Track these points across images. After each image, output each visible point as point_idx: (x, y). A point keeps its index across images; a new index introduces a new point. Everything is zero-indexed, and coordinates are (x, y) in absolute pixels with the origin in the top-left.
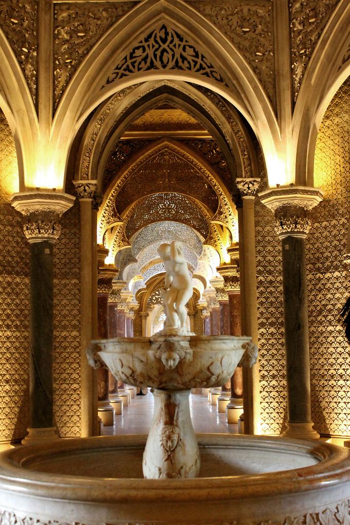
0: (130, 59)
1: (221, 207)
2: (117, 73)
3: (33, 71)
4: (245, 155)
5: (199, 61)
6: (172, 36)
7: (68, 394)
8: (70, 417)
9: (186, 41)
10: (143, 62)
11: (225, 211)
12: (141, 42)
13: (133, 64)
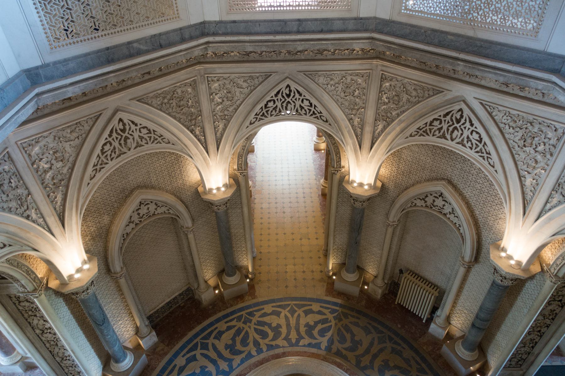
0: (265, 109)
2: (257, 118)
5: (313, 109)
6: (294, 93)
9: (304, 96)
10: (274, 111)
12: (272, 97)
13: (267, 112)
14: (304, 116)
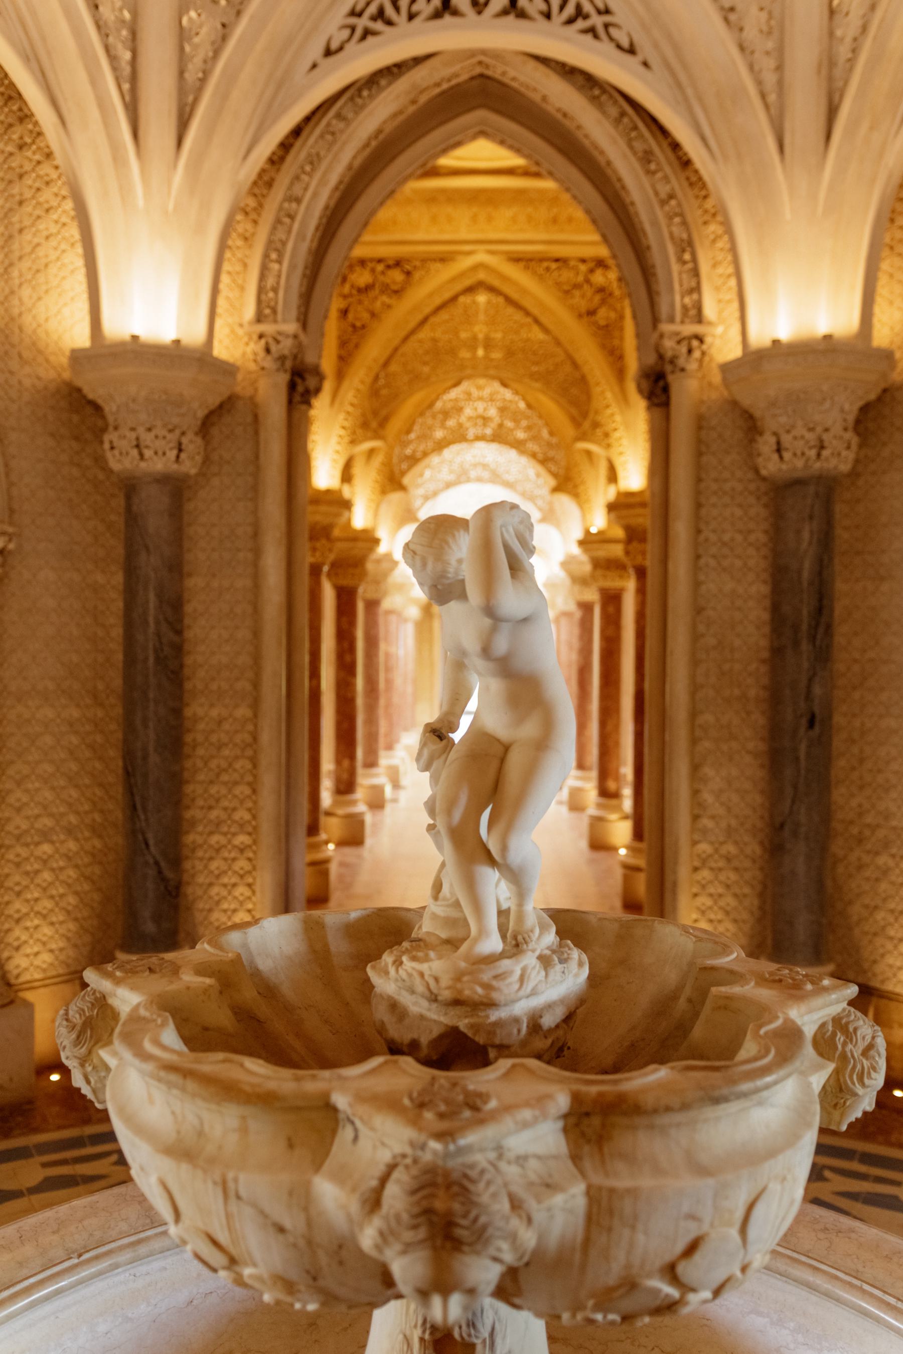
2: (353, 29)
3: (121, 10)
4: (685, 263)
7: (225, 859)
8: (229, 913)
14: (541, 21)
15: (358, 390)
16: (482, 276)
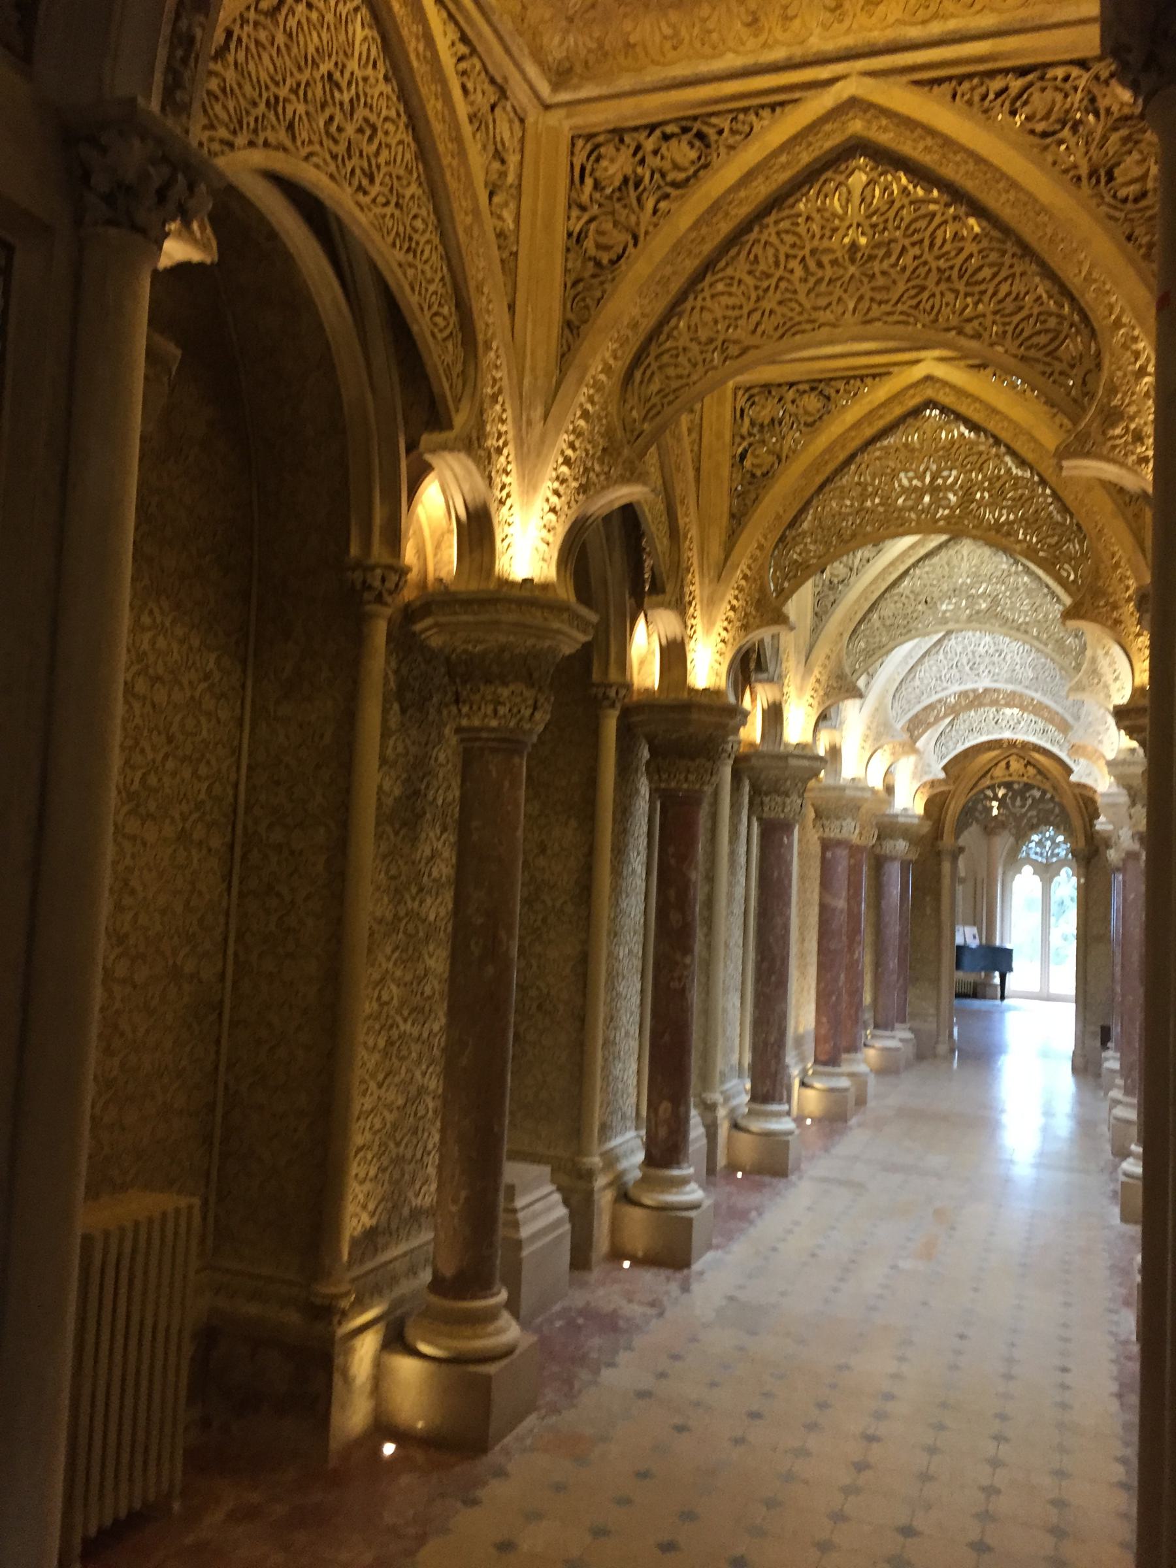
1: (1112, 390)
11: (1132, 409)
15: (598, 386)
16: (856, 126)
